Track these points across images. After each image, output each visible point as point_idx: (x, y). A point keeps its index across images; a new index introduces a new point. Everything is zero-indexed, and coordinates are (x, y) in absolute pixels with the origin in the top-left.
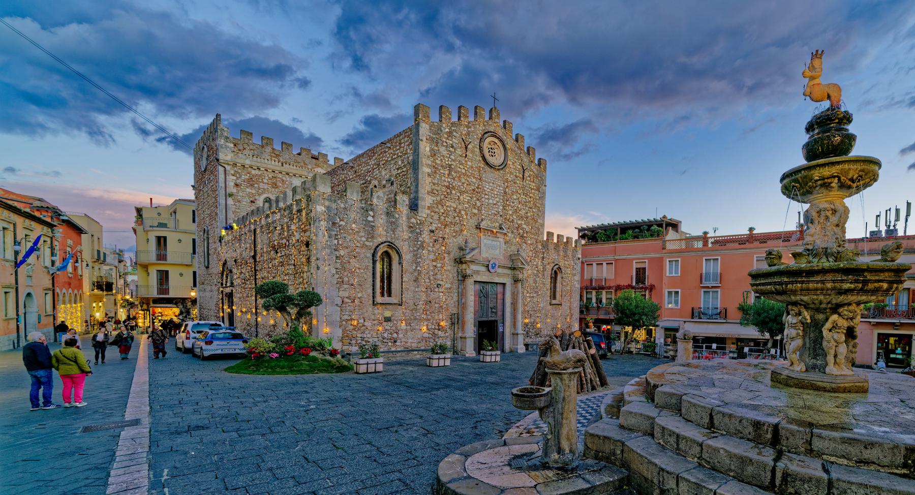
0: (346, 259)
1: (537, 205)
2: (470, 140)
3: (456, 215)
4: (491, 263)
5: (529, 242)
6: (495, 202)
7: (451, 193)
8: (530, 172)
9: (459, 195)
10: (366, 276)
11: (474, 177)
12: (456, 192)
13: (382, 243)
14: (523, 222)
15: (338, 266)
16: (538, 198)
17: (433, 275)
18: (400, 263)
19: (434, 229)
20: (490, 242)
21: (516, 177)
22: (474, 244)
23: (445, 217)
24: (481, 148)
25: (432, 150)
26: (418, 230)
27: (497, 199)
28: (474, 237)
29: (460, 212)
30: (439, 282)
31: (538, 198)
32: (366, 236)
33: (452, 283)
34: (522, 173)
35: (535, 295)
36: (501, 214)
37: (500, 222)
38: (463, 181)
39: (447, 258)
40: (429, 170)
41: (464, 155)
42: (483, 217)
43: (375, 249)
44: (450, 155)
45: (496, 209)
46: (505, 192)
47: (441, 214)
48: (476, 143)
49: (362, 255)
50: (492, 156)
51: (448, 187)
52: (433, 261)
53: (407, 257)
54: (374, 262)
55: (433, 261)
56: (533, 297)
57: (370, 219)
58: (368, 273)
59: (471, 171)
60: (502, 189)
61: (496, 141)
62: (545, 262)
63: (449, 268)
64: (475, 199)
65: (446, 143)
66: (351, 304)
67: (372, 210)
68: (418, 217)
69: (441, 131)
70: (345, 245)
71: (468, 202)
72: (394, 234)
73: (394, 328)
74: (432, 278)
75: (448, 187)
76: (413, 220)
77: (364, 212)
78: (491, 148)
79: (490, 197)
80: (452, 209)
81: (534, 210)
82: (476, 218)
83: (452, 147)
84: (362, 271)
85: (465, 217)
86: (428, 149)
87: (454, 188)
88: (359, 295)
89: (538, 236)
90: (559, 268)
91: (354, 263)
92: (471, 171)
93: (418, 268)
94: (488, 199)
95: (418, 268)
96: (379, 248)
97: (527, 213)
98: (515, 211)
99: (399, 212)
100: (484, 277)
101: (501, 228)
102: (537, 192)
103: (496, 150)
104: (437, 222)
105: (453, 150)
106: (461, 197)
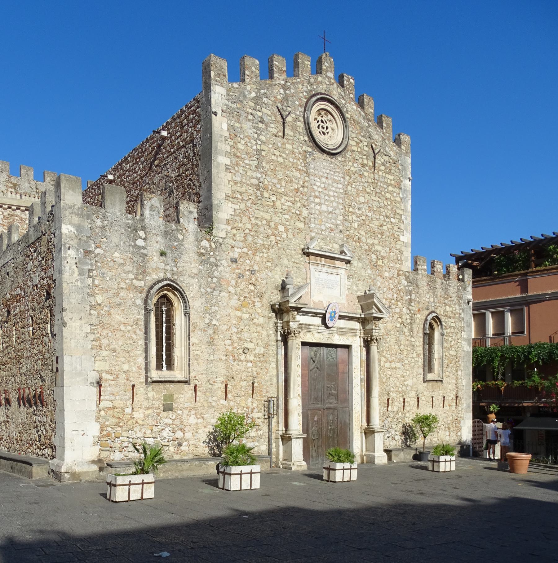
0: (105, 309)
1: (398, 211)
5: (386, 274)
6: (330, 209)
7: (262, 196)
8: (384, 157)
9: (274, 198)
10: (134, 336)
13: (159, 282)
14: (376, 242)
15: (94, 320)
16: (398, 199)
17: (237, 333)
18: (186, 314)
19: (236, 256)
21: (363, 165)
22: (299, 280)
25: (231, 128)
26: (212, 260)
27: (335, 204)
28: (299, 269)
29: (276, 228)
30: (246, 345)
31: (398, 199)
34: (372, 159)
35: (398, 365)
36: (341, 228)
37: (340, 242)
38: (280, 175)
39: (258, 305)
40: (227, 161)
42: (313, 234)
43: (149, 292)
47: (247, 231)
49: (129, 303)
50: (324, 133)
51: (258, 187)
54: (147, 312)
56: (395, 368)
57: (140, 242)
59: (291, 160)
60: (340, 186)
62: (414, 308)
63: (261, 320)
64: (299, 205)
66: (113, 382)
67: (143, 228)
69: (245, 96)
70: (103, 286)
71: (289, 211)
73: (177, 422)
77: (131, 232)
79: (323, 201)
80: (264, 222)
81: (393, 220)
82: (301, 236)
84: (129, 328)
85: (284, 235)
86: (225, 126)
87: (265, 188)
88: (126, 367)
89: (401, 264)
90: (437, 319)
91: (117, 316)
92: (291, 160)
93: (214, 322)
94: (320, 204)
95: (214, 322)
96: (152, 292)
97: (382, 226)
98: (364, 223)
101: (342, 252)
102: (397, 190)
104: (241, 245)
106: (278, 204)
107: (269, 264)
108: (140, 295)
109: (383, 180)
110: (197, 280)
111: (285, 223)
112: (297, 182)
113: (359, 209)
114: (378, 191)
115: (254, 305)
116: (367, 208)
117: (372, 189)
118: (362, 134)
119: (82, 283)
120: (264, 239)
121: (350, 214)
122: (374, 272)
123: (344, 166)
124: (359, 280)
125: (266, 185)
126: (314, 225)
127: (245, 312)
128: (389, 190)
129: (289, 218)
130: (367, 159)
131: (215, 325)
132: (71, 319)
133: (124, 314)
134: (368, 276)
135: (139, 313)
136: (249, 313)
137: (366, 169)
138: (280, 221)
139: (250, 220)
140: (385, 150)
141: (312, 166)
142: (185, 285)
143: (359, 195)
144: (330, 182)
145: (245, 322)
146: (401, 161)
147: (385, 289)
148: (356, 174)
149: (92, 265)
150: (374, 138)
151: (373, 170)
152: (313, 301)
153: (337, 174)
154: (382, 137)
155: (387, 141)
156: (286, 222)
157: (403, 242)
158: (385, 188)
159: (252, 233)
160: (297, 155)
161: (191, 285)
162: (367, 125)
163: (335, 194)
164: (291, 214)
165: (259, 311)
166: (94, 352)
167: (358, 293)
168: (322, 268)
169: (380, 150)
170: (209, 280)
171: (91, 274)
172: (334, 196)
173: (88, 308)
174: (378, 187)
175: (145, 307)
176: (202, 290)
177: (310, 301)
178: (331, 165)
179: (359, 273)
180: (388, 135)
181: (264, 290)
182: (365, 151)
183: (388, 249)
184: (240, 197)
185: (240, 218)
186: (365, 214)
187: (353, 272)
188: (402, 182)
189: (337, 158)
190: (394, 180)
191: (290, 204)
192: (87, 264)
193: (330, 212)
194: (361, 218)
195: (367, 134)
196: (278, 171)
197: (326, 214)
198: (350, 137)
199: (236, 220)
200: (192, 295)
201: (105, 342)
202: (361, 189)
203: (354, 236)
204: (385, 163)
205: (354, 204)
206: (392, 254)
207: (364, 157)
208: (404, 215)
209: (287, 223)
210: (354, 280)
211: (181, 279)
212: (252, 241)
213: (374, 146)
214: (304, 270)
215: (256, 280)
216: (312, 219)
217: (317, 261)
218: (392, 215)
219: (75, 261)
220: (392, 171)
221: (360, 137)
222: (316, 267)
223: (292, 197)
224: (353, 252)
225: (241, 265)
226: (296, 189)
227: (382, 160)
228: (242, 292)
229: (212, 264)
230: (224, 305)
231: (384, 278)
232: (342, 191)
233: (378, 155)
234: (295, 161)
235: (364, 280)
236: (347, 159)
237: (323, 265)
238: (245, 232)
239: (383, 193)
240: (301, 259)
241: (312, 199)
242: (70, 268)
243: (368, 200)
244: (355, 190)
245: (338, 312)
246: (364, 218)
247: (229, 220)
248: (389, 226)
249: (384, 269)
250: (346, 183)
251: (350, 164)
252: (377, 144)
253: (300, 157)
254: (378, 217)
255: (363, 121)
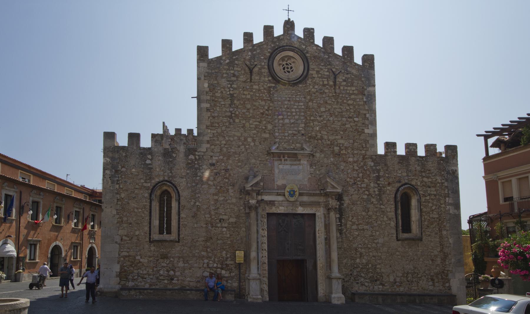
1: (362, 112)
2: (256, 63)
3: (241, 143)
4: (287, 189)
5: (351, 159)
6: (292, 121)
7: (234, 122)
8: (346, 76)
11: (262, 100)
12: (240, 120)
13: (159, 182)
17: (214, 210)
18: (179, 201)
19: (214, 162)
20: (287, 167)
23: (227, 148)
24: (270, 68)
26: (196, 166)
27: (297, 117)
28: (265, 164)
29: (246, 139)
31: (362, 103)
32: (145, 178)
33: (238, 217)
36: (303, 132)
38: (249, 106)
39: (231, 191)
41: (249, 80)
42: (277, 140)
43: (153, 189)
44: (231, 85)
45: (296, 129)
46: (308, 107)
48: (263, 64)
51: (230, 117)
52: (214, 195)
53: (185, 194)
55: (214, 195)
58: (145, 212)
59: (257, 95)
60: (302, 104)
61: (291, 54)
63: (234, 200)
65: (226, 73)
68: (197, 153)
71: (256, 127)
72: (171, 172)
74: (213, 213)
75: (230, 117)
76: (191, 157)
78: (287, 64)
80: (236, 138)
81: (356, 119)
83: (234, 75)
84: (140, 210)
87: (237, 116)
91: (133, 204)
92: (257, 95)
93: (197, 204)
95: (197, 204)
99: (177, 152)
100: (281, 208)
101: (303, 149)
102: (361, 96)
103: (293, 65)
104: (218, 154)
105: (235, 79)
106: (247, 124)
107: (240, 164)
108: (147, 191)
109: (344, 92)
110: (185, 179)
111: (252, 136)
112: (263, 108)
113: (320, 117)
114: (340, 101)
115: (228, 191)
116: (329, 114)
117: (334, 100)
118: (322, 64)
119: (113, 187)
120: (236, 148)
121: (311, 121)
122: (337, 159)
123: (305, 89)
124: (322, 166)
125: (237, 115)
126: (278, 134)
127: (220, 196)
128: (352, 97)
129: (256, 132)
130: (328, 80)
131: (198, 206)
132: (106, 207)
133: (137, 202)
134: (331, 163)
135: (146, 202)
136: (224, 196)
137: (327, 88)
138: (248, 135)
139: (225, 138)
140: (347, 70)
141: (275, 95)
142: (176, 183)
143: (319, 107)
144: (292, 103)
145: (221, 202)
146: (364, 74)
147: (349, 171)
148: (317, 94)
149: (119, 177)
150: (335, 64)
151: (334, 87)
152: (277, 184)
153: (298, 96)
154: (343, 61)
155: (348, 64)
156: (254, 135)
157: (369, 134)
158: (347, 98)
159: (226, 146)
160: (262, 90)
161: (181, 183)
162: (327, 57)
163: (297, 110)
164: (257, 130)
165: (232, 194)
166: (118, 224)
167: (321, 176)
168: (286, 162)
169: (341, 72)
170: (194, 178)
171: (118, 182)
172: (296, 112)
173: (116, 201)
174: (340, 98)
175: (150, 198)
176: (189, 185)
177: (274, 185)
178: (293, 92)
179: (321, 161)
180: (349, 59)
181: (236, 181)
182: (325, 75)
183: (351, 141)
184: (217, 125)
185: (217, 138)
186: (327, 119)
187: (316, 161)
188: (366, 89)
189: (298, 85)
190: (356, 90)
191: (257, 123)
192: (116, 177)
193: (293, 123)
194: (322, 122)
195: (328, 63)
196: (247, 104)
197: (288, 125)
198: (310, 69)
199: (214, 140)
200: (182, 188)
201: (125, 219)
202: (322, 102)
203: (317, 136)
204: (346, 79)
205: (315, 114)
206: (356, 144)
207: (324, 79)
208: (368, 113)
209: (255, 136)
210: (316, 167)
211: (175, 180)
212: (227, 151)
213: (334, 70)
214: (270, 165)
215: (230, 175)
216: (276, 130)
217: (280, 157)
218: (355, 116)
219: (109, 176)
220: (354, 84)
221: (321, 67)
222: (280, 162)
223: (258, 119)
224: (315, 148)
225: (218, 167)
226: (261, 113)
227: (344, 78)
228: (218, 184)
229: (196, 169)
230: (205, 193)
231: (348, 162)
232: (303, 107)
233: (338, 75)
234: (261, 95)
235: (327, 166)
236: (308, 84)
237: (286, 160)
238: (222, 146)
239: (345, 101)
240: (267, 158)
241: (276, 117)
242: (107, 180)
243: (329, 109)
244: (316, 104)
245: (298, 190)
246: (325, 122)
247: (209, 141)
248: (352, 124)
249: (348, 156)
250: (307, 101)
251: (311, 87)
252: (338, 68)
253: (266, 92)
254: (340, 119)
255: (323, 55)
